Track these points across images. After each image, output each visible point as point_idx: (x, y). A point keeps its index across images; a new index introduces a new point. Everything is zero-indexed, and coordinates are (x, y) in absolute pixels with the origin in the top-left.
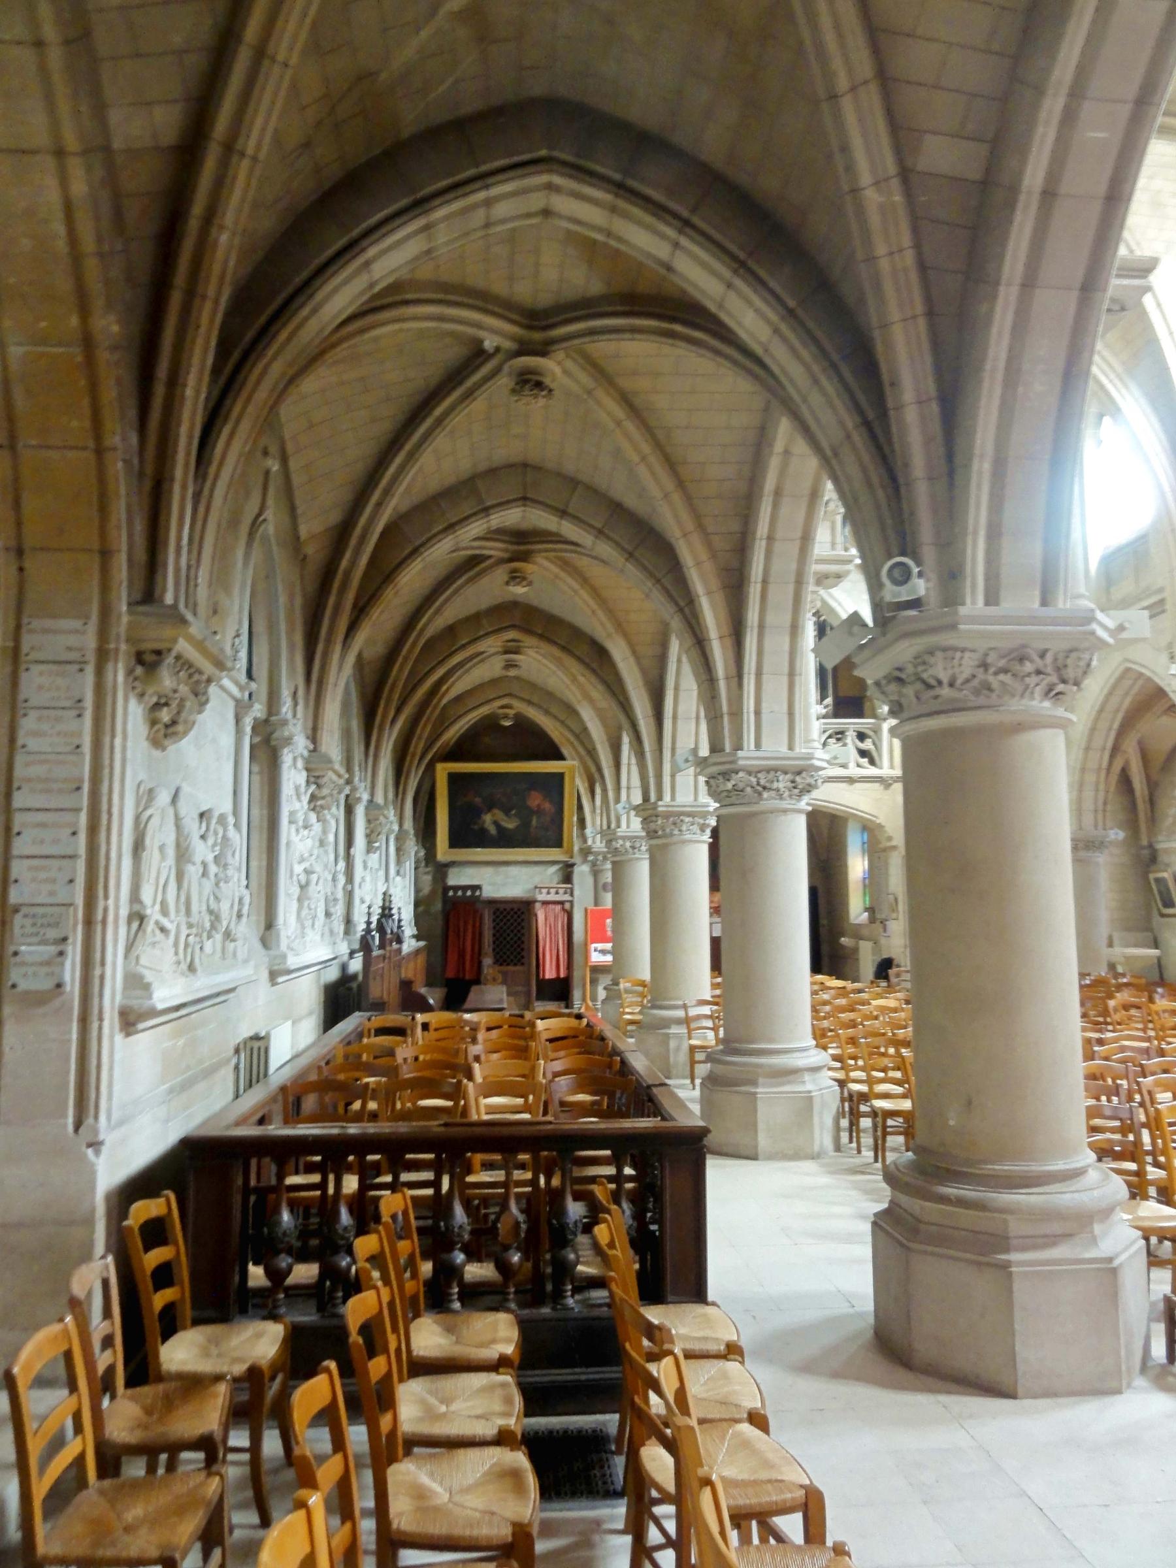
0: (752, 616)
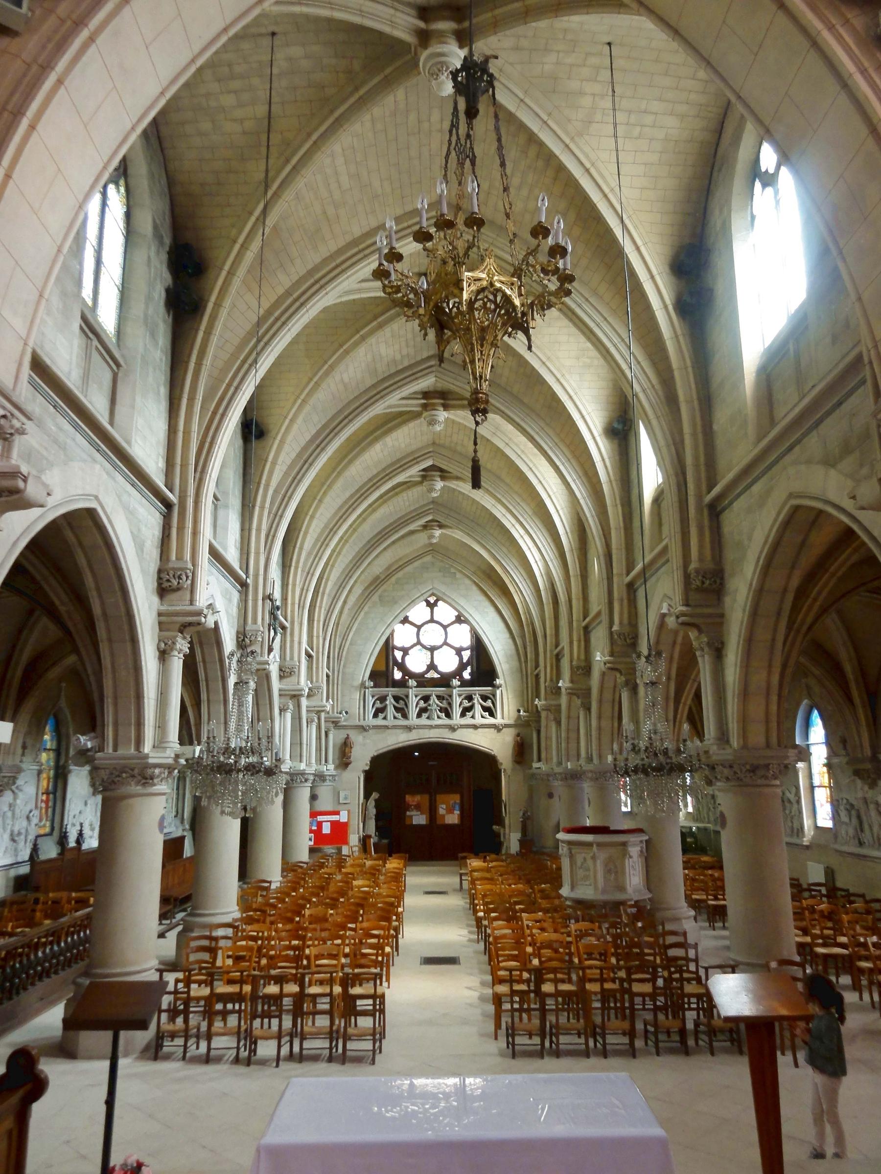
0: (204, 696)
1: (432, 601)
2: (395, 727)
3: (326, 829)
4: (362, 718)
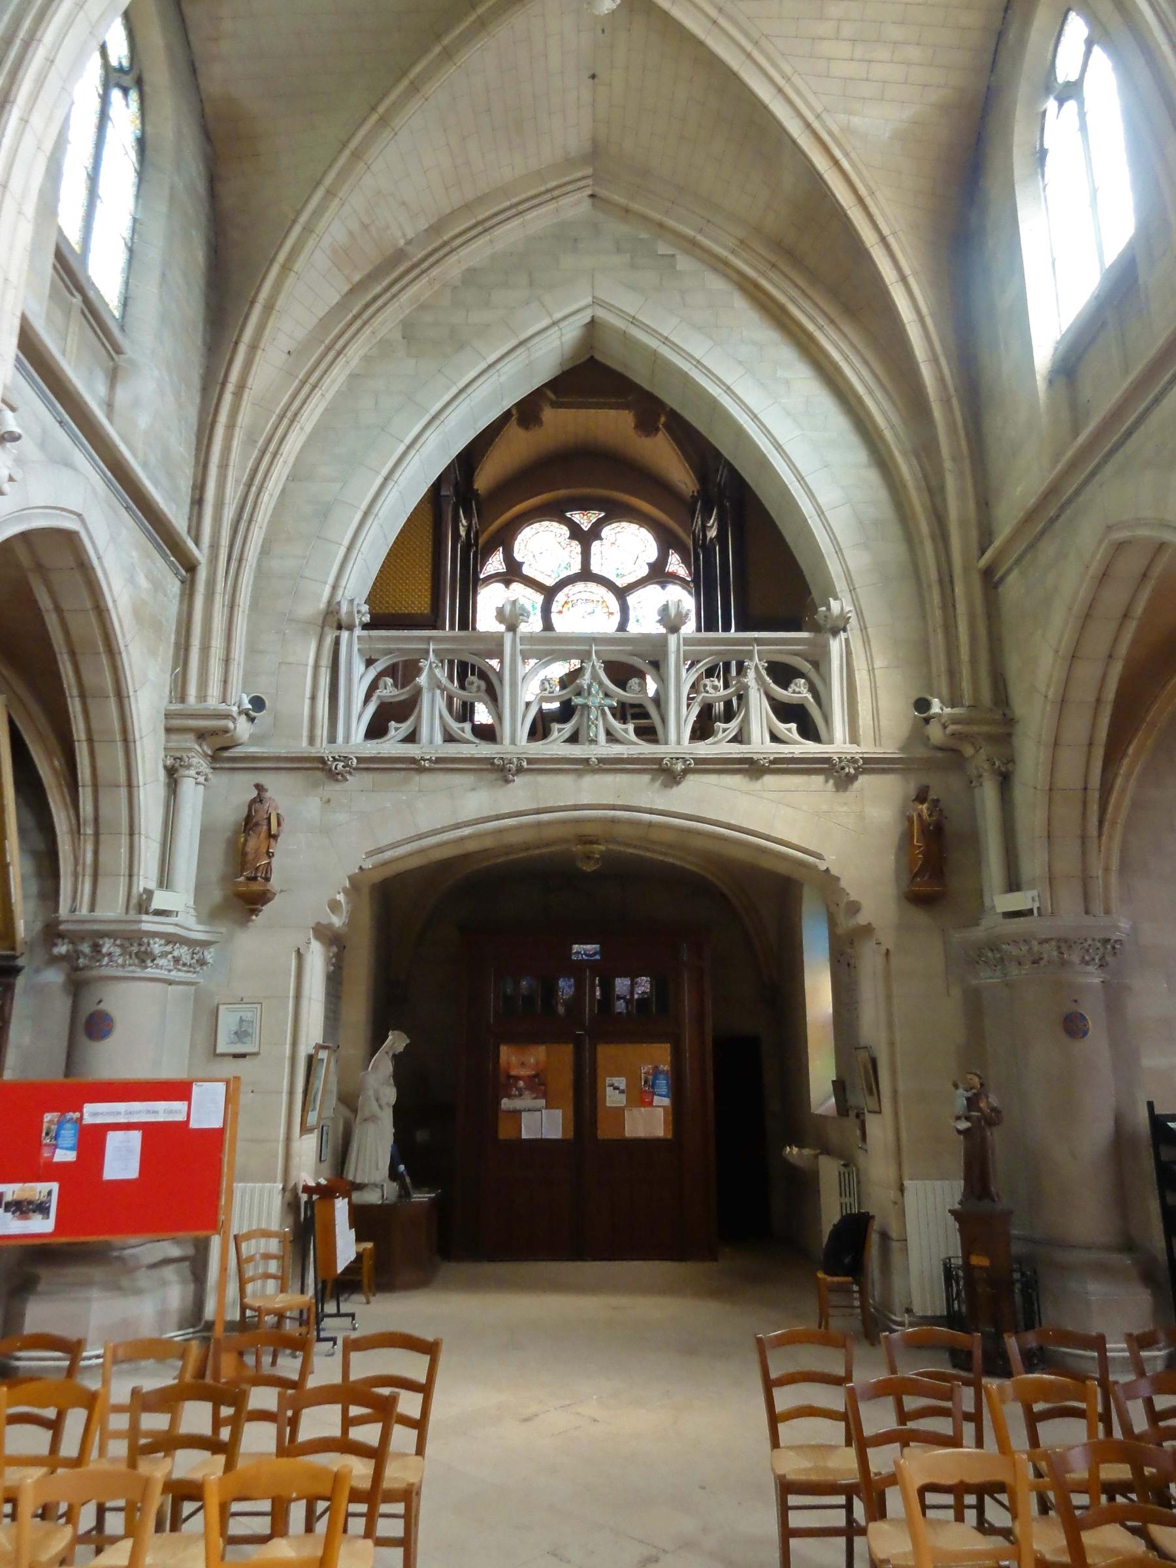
1: (586, 526)
2: (443, 765)
3: (122, 1160)
4: (322, 731)
